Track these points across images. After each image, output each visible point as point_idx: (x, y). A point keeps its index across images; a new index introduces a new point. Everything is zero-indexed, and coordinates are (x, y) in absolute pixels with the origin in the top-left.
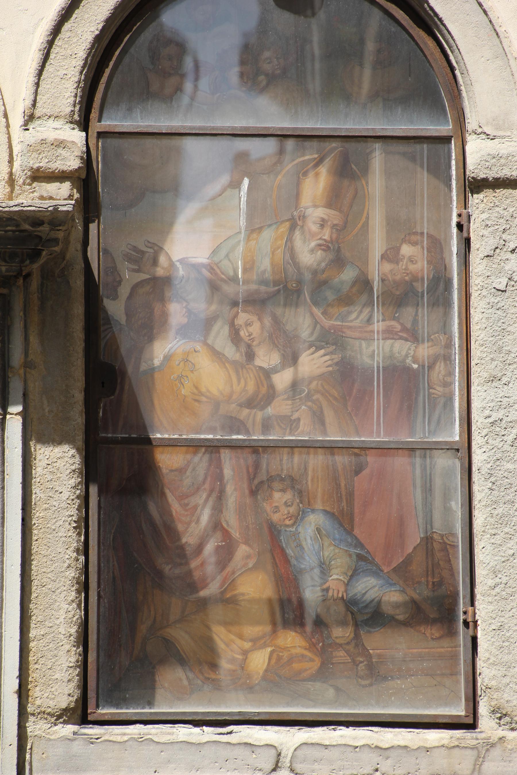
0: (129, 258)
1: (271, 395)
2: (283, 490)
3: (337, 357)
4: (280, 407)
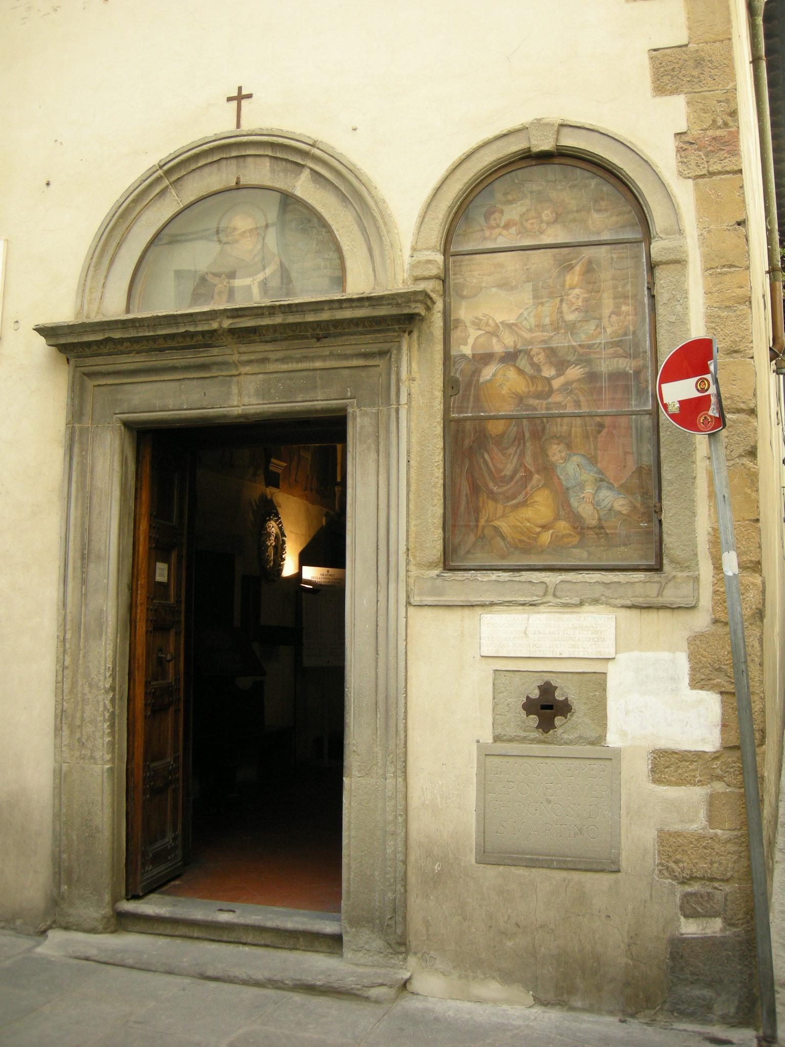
0: (473, 323)
1: (551, 392)
2: (558, 444)
3: (587, 370)
4: (556, 398)
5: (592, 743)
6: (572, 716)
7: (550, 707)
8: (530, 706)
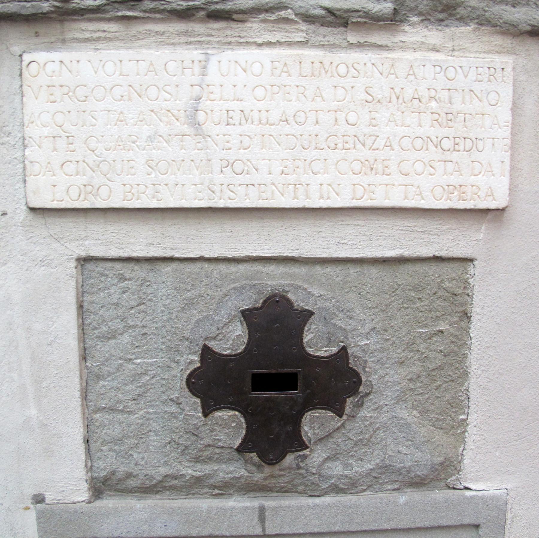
5: (419, 483)
6: (360, 405)
7: (287, 382)
8: (214, 381)
